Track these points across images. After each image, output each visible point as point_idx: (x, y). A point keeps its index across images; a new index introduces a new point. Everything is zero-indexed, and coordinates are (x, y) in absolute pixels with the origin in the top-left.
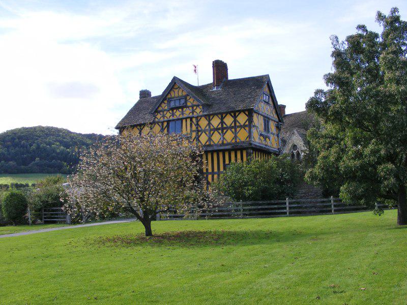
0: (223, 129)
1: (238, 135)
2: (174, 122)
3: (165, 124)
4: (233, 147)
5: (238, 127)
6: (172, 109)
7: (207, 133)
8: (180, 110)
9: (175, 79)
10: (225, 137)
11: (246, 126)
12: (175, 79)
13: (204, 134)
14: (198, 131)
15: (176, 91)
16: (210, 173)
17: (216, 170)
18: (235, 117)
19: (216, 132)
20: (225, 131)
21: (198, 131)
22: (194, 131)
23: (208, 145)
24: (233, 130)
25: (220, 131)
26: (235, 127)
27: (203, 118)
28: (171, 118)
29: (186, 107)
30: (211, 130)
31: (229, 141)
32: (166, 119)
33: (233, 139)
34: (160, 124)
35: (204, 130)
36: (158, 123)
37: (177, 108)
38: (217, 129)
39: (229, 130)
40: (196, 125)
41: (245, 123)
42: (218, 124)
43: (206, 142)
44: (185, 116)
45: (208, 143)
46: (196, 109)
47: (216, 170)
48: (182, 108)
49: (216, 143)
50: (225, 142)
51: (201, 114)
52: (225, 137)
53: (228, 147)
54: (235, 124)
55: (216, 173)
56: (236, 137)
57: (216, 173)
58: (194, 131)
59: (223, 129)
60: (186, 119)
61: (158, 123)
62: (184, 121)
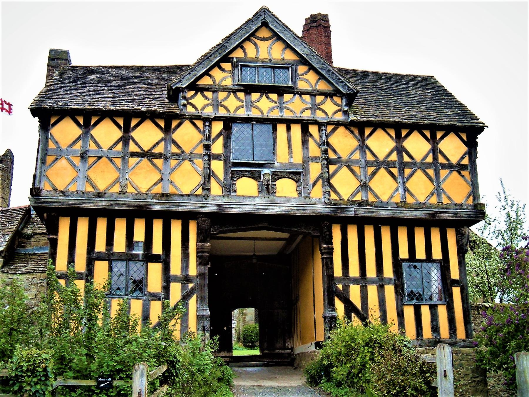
0: (403, 166)
1: (443, 186)
2: (246, 129)
3: (218, 127)
4: (433, 215)
5: (443, 166)
6: (248, 89)
7: (356, 169)
8: (274, 96)
9: (264, 11)
10: (407, 185)
11: (464, 167)
12: (264, 11)
13: (345, 170)
14: (330, 162)
15: (263, 46)
16: (355, 281)
17: (371, 272)
18: (434, 141)
19: (382, 171)
20: (407, 171)
21: (330, 162)
22: (314, 159)
23: (360, 203)
24: (431, 172)
25: (395, 171)
26: (436, 166)
27: (341, 130)
28: (242, 113)
29: (293, 91)
30: (368, 164)
31: (422, 199)
32: (222, 112)
33: (432, 194)
34: (199, 123)
35: (347, 162)
36: (192, 119)
37: (264, 90)
38: (387, 165)
39: (419, 173)
40: (319, 145)
41: (462, 158)
42: (388, 150)
43: (354, 195)
44: (287, 115)
45: (358, 198)
46: (322, 103)
47: (371, 272)
48: (281, 91)
49: (385, 198)
50: (410, 200)
51: (339, 117)
52: (407, 185)
53: (420, 214)
54: (435, 158)
55: (372, 282)
56: (438, 191)
57: (372, 282)
58: (314, 159)
59: (403, 166)
60: (289, 123)
61: (192, 119)
62: (281, 129)
